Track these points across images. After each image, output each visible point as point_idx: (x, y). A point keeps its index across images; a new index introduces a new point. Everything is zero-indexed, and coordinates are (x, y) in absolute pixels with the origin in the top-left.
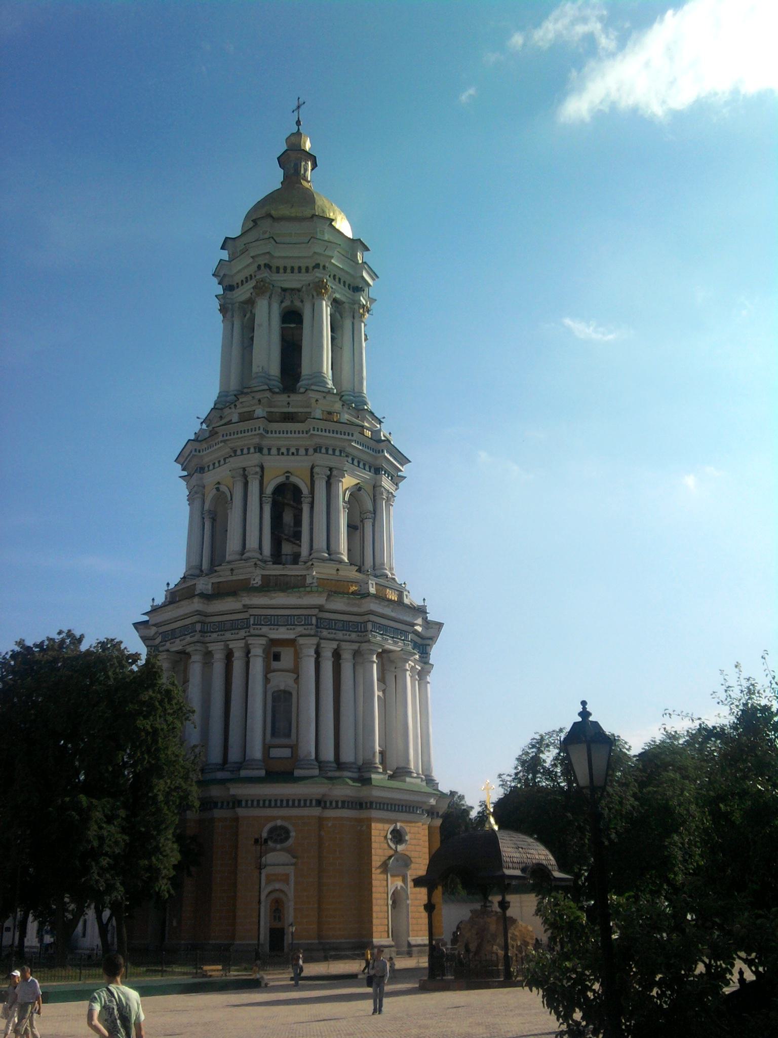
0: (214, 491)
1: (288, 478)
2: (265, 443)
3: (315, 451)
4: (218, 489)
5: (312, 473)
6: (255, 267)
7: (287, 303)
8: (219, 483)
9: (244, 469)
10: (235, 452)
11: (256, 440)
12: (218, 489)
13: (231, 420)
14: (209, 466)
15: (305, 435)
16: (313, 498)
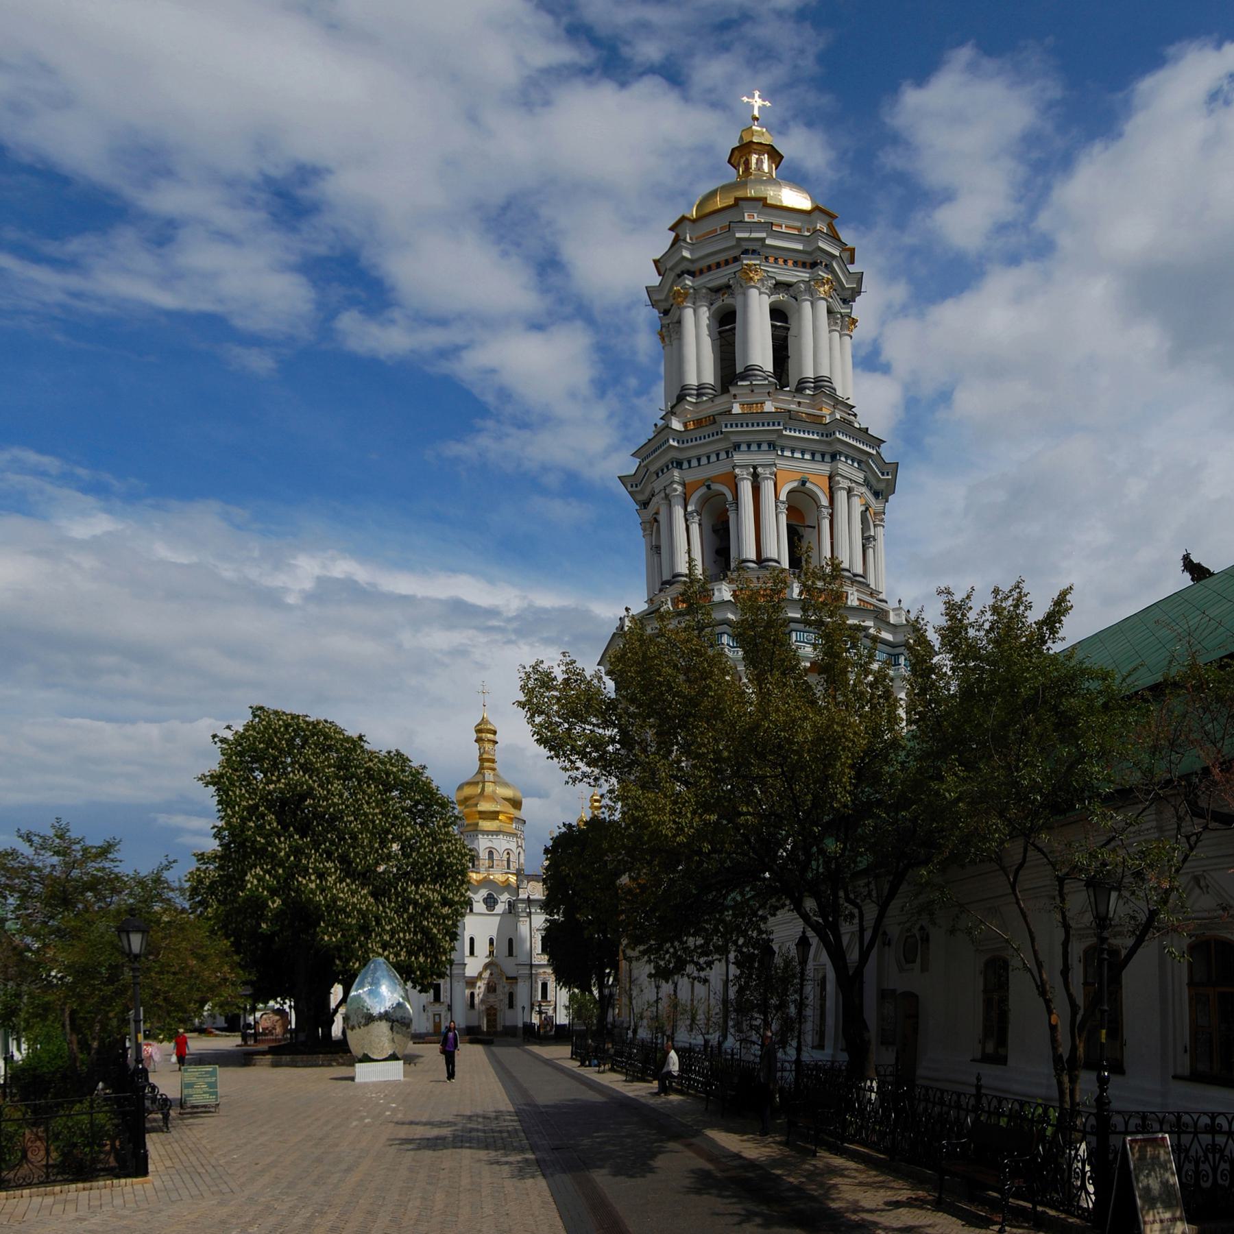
0: (704, 489)
1: (804, 483)
2: (780, 442)
3: (834, 457)
4: (709, 487)
5: (830, 483)
6: (736, 253)
7: (773, 298)
8: (709, 479)
9: (755, 468)
10: (739, 448)
11: (773, 437)
12: (709, 487)
13: (731, 411)
14: (689, 462)
15: (824, 438)
16: (832, 509)
